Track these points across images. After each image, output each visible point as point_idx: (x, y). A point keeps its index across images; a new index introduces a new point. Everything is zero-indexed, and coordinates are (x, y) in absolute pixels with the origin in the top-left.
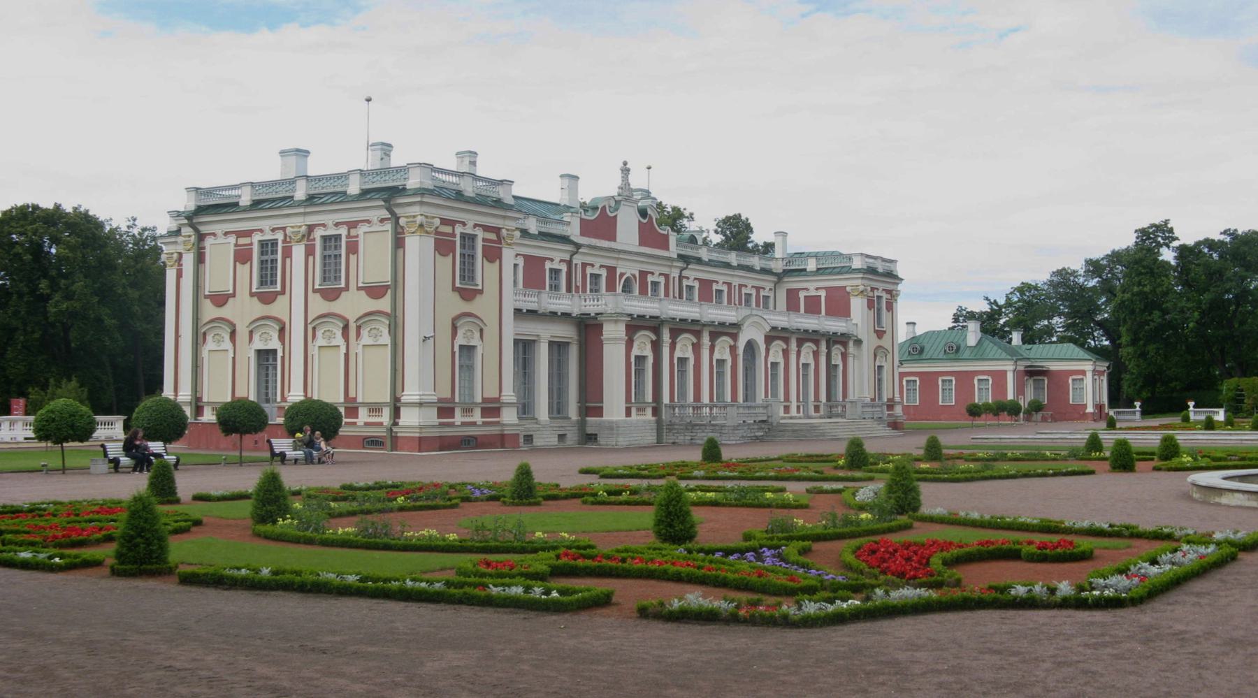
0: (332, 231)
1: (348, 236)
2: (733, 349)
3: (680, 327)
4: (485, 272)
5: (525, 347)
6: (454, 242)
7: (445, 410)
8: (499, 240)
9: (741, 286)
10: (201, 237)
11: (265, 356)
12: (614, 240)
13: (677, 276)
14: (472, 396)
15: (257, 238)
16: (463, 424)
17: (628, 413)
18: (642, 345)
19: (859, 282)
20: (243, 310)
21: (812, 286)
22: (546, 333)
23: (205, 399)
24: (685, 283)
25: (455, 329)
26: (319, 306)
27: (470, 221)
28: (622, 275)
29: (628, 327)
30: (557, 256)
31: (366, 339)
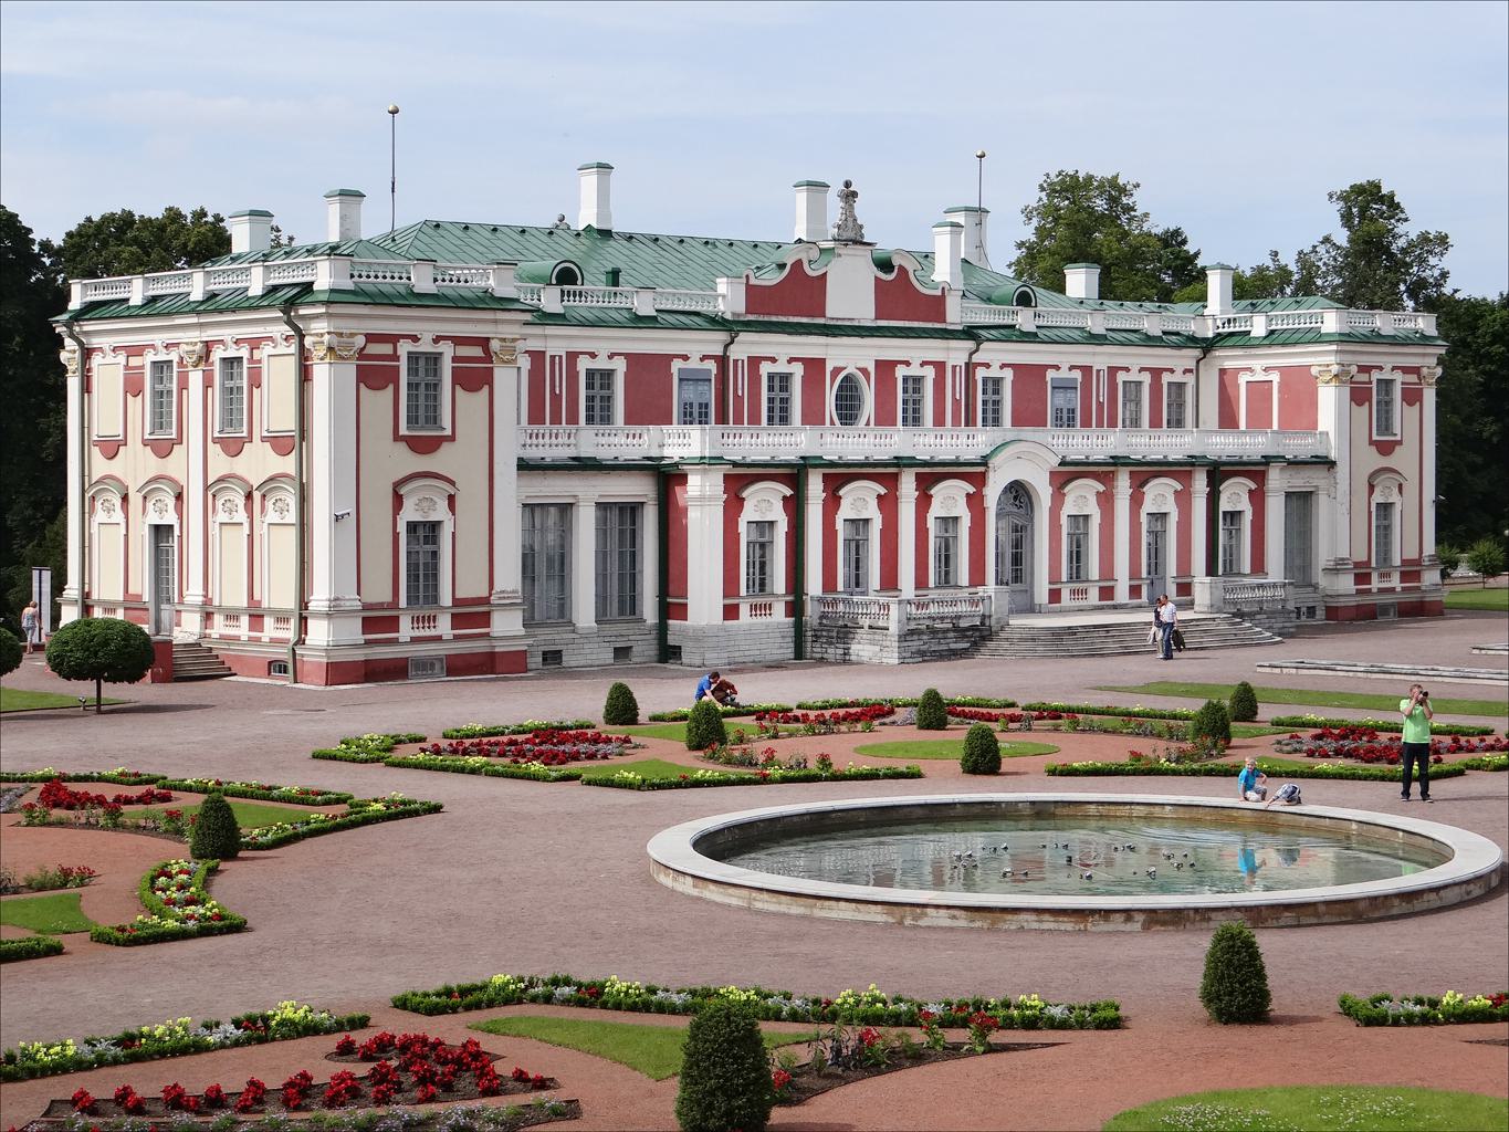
0: (231, 353)
1: (251, 359)
2: (975, 502)
3: (839, 476)
4: (461, 410)
5: (549, 519)
6: (398, 367)
7: (378, 621)
8: (488, 357)
9: (1113, 371)
10: (87, 353)
11: (161, 532)
14: (434, 599)
15: (150, 357)
16: (414, 640)
17: (731, 612)
18: (765, 503)
19: (1331, 359)
20: (135, 465)
21: (1258, 364)
22: (587, 493)
23: (95, 596)
24: (980, 373)
25: (398, 501)
26: (220, 464)
27: (426, 329)
28: (837, 371)
29: (727, 477)
31: (272, 516)
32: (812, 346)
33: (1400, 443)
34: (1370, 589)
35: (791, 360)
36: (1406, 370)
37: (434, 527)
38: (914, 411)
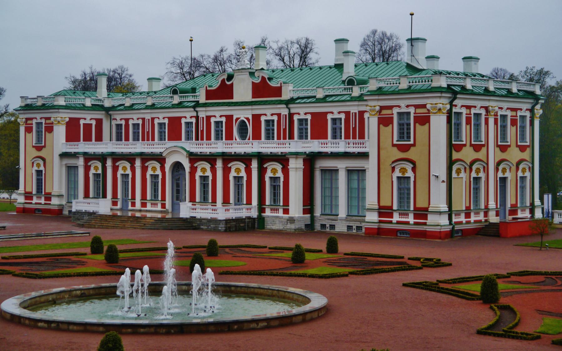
2: (163, 169)
12: (232, 98)
13: (287, 113)
14: (42, 192)
16: (36, 203)
18: (96, 167)
24: (296, 118)
25: (33, 163)
28: (237, 119)
30: (188, 115)
32: (227, 110)
33: (414, 145)
34: (426, 223)
35: (221, 116)
36: (417, 107)
37: (42, 171)
38: (269, 134)
